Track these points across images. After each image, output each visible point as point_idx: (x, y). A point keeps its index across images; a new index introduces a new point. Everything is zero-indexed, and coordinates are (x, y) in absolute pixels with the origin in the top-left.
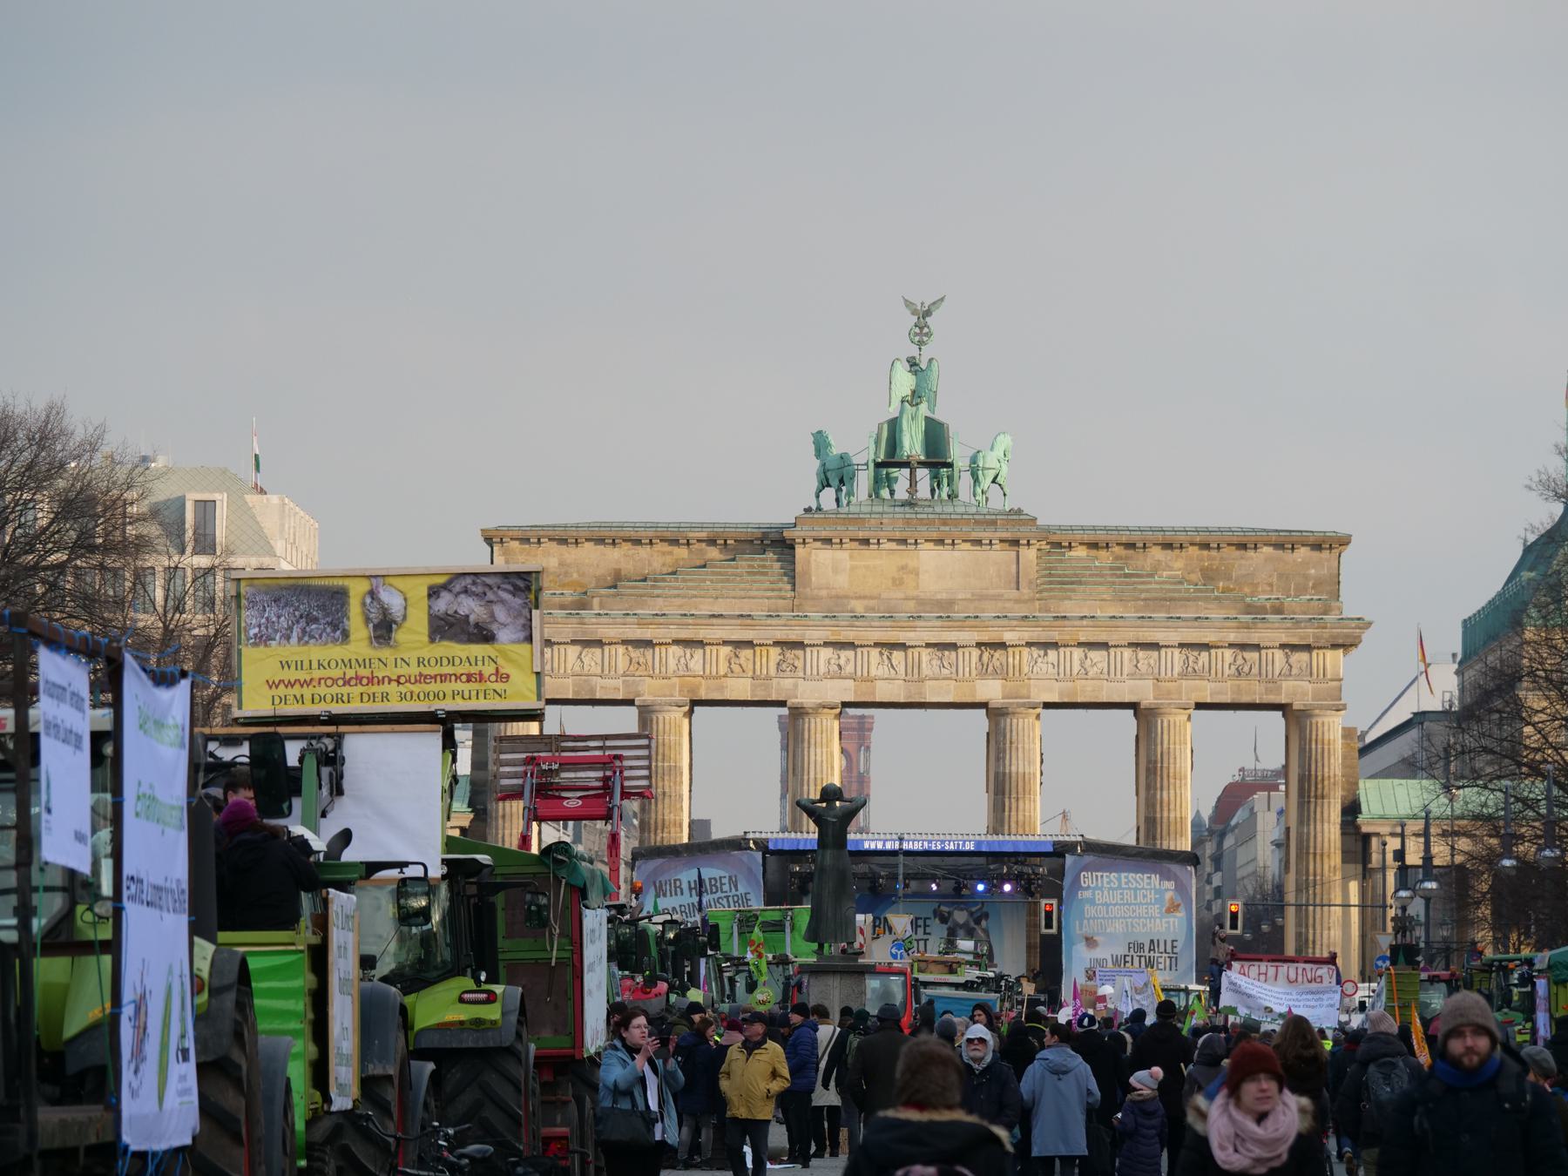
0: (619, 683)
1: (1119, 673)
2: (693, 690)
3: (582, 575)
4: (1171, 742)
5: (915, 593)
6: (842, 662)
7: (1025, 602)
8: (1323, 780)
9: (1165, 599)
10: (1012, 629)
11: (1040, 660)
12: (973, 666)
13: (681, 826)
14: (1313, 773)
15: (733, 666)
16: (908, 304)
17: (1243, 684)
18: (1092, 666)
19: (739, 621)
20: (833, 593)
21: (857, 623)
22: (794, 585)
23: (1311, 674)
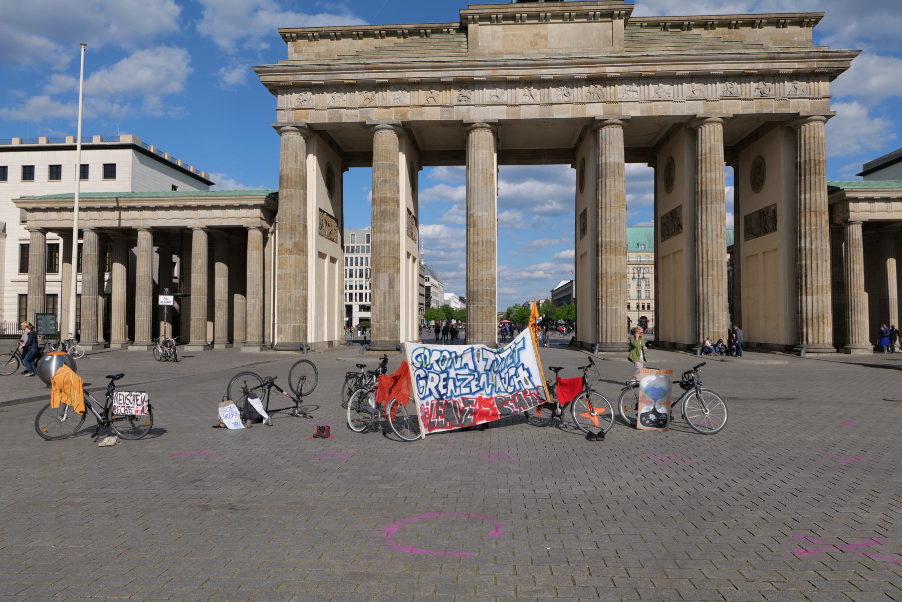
0: (357, 112)
1: (680, 96)
4: (716, 140)
5: (547, 50)
8: (819, 162)
9: (709, 49)
10: (610, 63)
11: (628, 89)
12: (584, 94)
13: (397, 202)
14: (812, 158)
15: (430, 100)
19: (430, 64)
20: (492, 52)
21: (509, 63)
23: (810, 94)
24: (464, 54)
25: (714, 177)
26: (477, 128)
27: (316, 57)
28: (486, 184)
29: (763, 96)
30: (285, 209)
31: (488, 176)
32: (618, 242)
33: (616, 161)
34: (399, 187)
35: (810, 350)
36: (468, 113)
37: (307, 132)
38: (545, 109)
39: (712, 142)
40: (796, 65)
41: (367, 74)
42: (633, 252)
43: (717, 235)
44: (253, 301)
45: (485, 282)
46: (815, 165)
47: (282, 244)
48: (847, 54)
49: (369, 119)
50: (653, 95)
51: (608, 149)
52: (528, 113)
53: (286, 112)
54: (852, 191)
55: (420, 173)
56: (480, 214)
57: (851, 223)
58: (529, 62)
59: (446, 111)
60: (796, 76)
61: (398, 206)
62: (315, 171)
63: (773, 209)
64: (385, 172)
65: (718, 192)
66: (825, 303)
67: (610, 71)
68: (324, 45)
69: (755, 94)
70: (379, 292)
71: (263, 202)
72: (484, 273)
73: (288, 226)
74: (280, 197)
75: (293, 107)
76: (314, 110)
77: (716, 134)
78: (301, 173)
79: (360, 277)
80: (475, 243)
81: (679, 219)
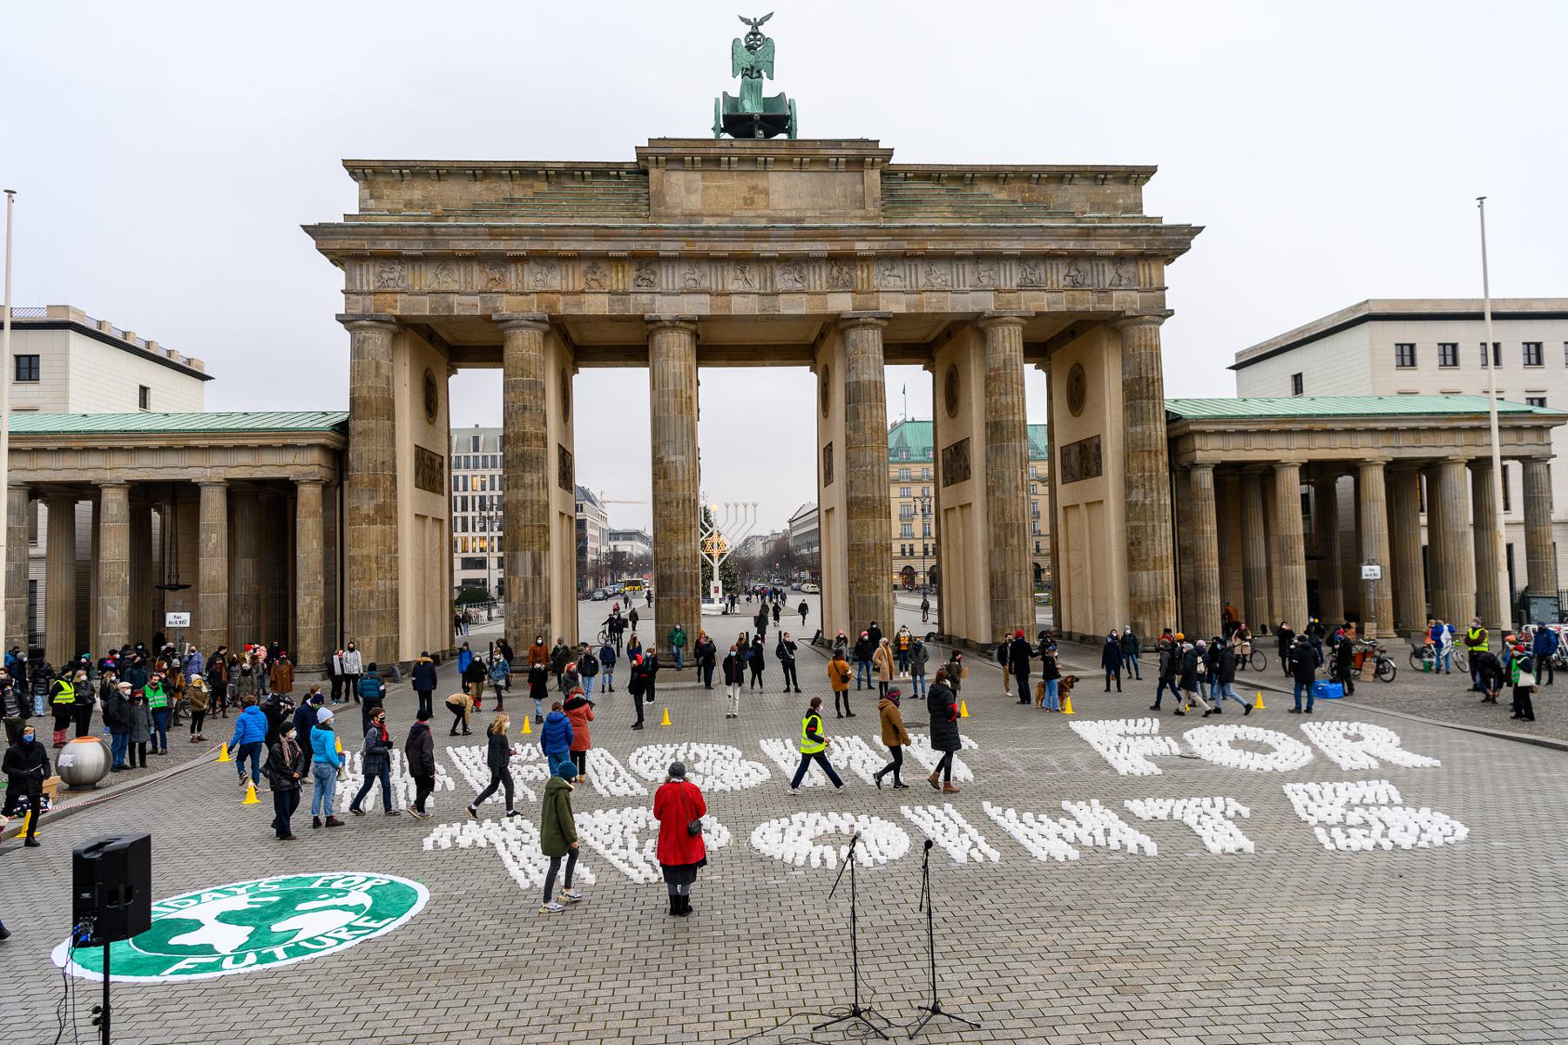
1: (961, 284)
2: (552, 306)
3: (447, 206)
4: (1013, 349)
5: (766, 212)
6: (696, 276)
7: (871, 219)
8: (1153, 382)
9: (1002, 216)
11: (887, 273)
12: (824, 278)
13: (544, 439)
14: (1144, 375)
16: (743, 19)
17: (1077, 294)
18: (936, 278)
20: (687, 212)
22: (649, 205)
24: (643, 214)
25: (1011, 403)
26: (665, 327)
27: (405, 206)
28: (682, 412)
29: (1075, 286)
30: (362, 453)
31: (684, 400)
32: (877, 498)
33: (873, 378)
34: (545, 416)
35: (1147, 648)
36: (651, 304)
37: (392, 327)
38: (767, 301)
39: (1008, 353)
40: (1120, 246)
41: (492, 243)
42: (917, 462)
43: (1017, 487)
44: (308, 600)
45: (681, 563)
46: (1148, 386)
47: (358, 508)
48: (1186, 231)
49: (496, 310)
50: (922, 281)
51: (860, 361)
52: (742, 306)
53: (360, 297)
54: (1198, 421)
55: (575, 378)
56: (673, 458)
57: (1195, 465)
58: (743, 232)
59: (618, 300)
60: (1119, 258)
61: (545, 445)
62: (408, 386)
63: (1096, 441)
64: (523, 394)
65: (1018, 425)
66: (1165, 581)
67: (860, 246)
68: (417, 191)
69: (1066, 283)
70: (517, 581)
71: (322, 441)
72: (680, 548)
73: (367, 480)
74: (352, 432)
75: (372, 288)
76: (405, 295)
77: (1013, 340)
78: (386, 396)
79: (463, 510)
80: (667, 503)
81: (966, 459)
